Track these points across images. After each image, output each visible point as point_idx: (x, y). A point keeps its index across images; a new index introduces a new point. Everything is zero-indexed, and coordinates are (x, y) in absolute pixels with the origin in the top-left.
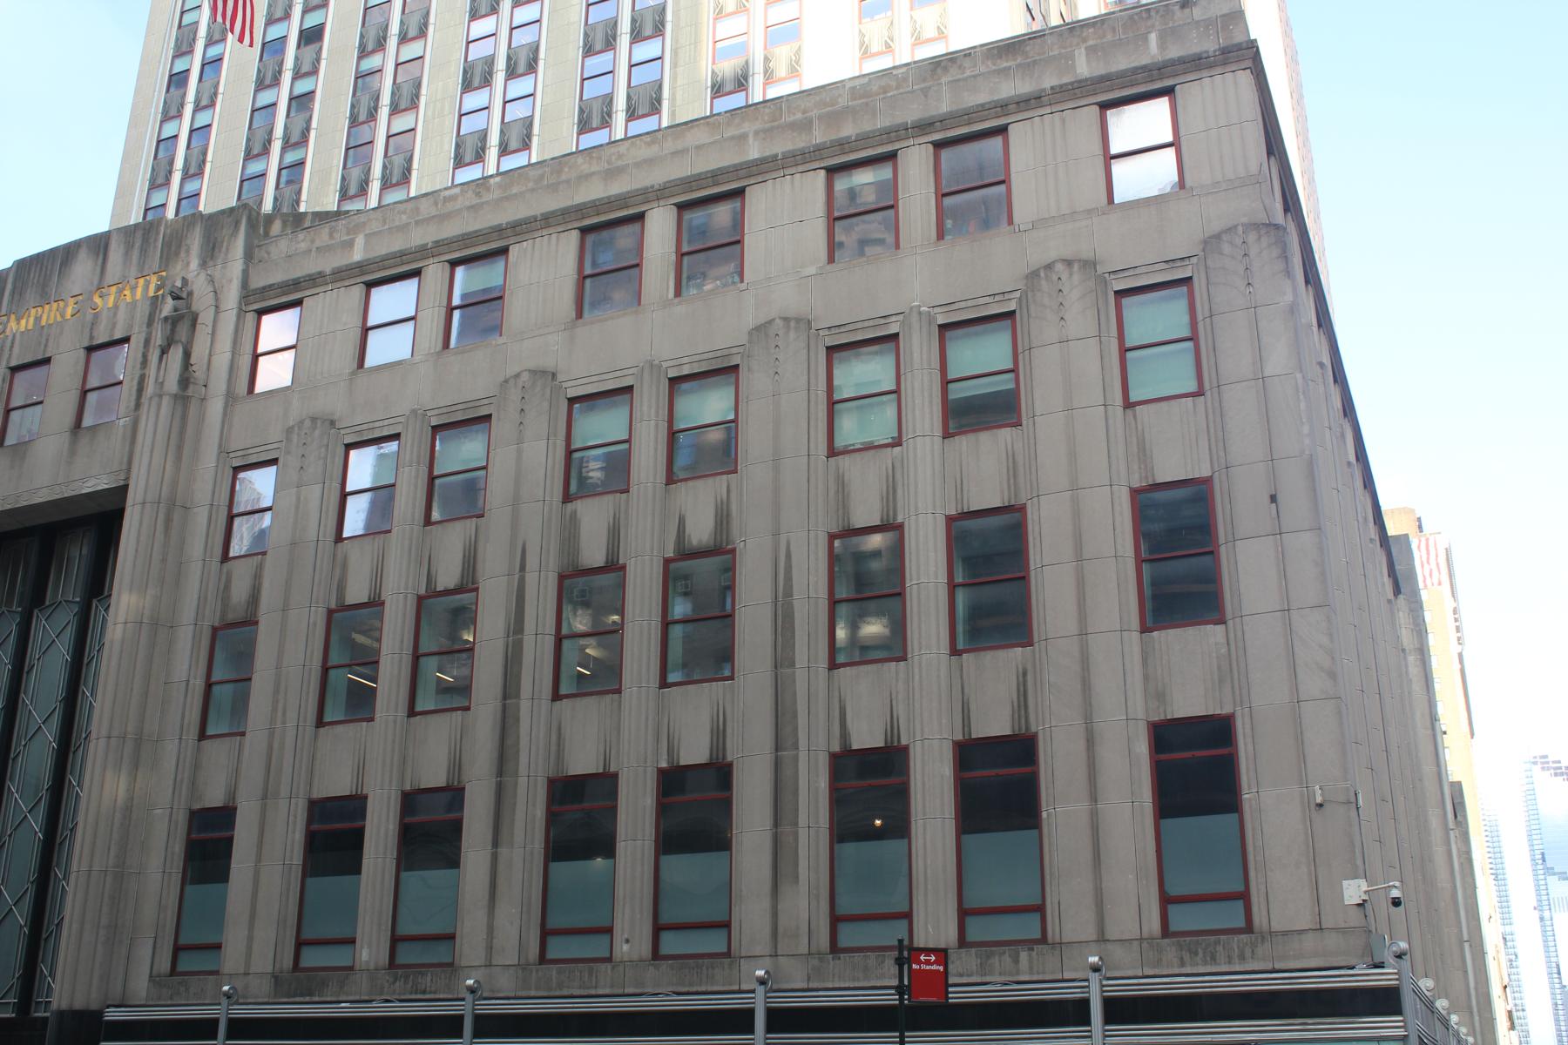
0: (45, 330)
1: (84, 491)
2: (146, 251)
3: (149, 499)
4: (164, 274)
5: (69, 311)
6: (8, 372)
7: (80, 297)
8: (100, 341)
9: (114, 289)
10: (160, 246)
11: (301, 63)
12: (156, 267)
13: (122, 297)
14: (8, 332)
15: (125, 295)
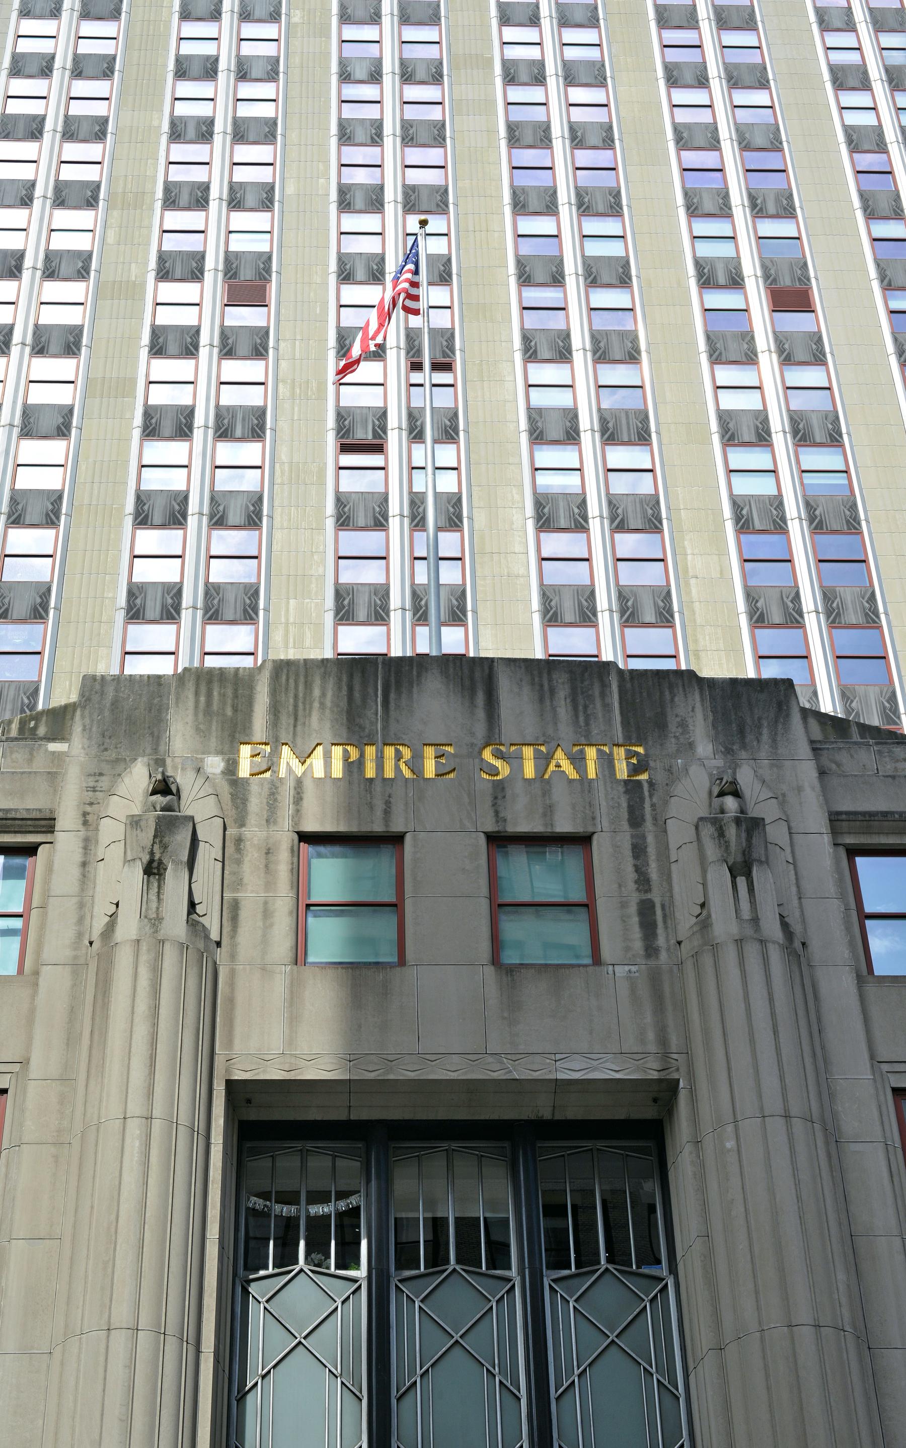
0: (378, 787)
1: (561, 1076)
2: (586, 707)
3: (794, 1111)
4: (640, 750)
5: (430, 769)
6: (296, 837)
7: (449, 749)
8: (524, 827)
9: (528, 752)
10: (616, 705)
11: (24, 510)
12: (618, 732)
13: (552, 767)
14: (282, 774)
15: (558, 766)
